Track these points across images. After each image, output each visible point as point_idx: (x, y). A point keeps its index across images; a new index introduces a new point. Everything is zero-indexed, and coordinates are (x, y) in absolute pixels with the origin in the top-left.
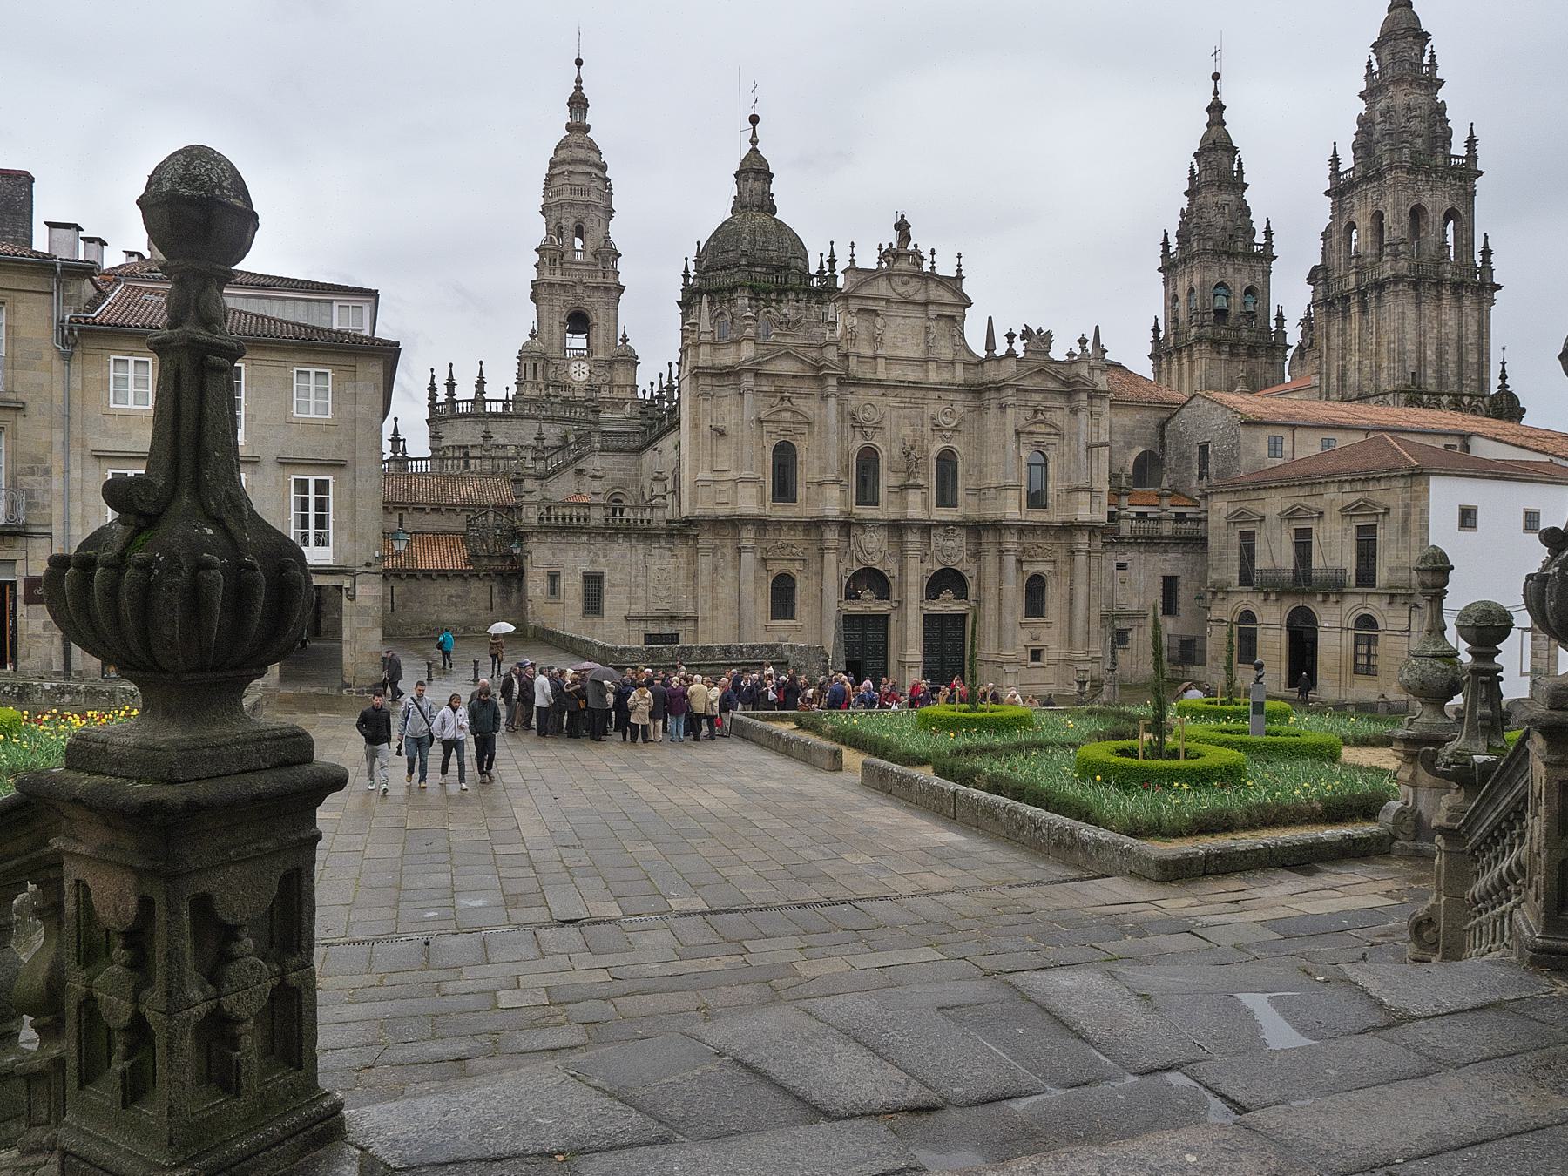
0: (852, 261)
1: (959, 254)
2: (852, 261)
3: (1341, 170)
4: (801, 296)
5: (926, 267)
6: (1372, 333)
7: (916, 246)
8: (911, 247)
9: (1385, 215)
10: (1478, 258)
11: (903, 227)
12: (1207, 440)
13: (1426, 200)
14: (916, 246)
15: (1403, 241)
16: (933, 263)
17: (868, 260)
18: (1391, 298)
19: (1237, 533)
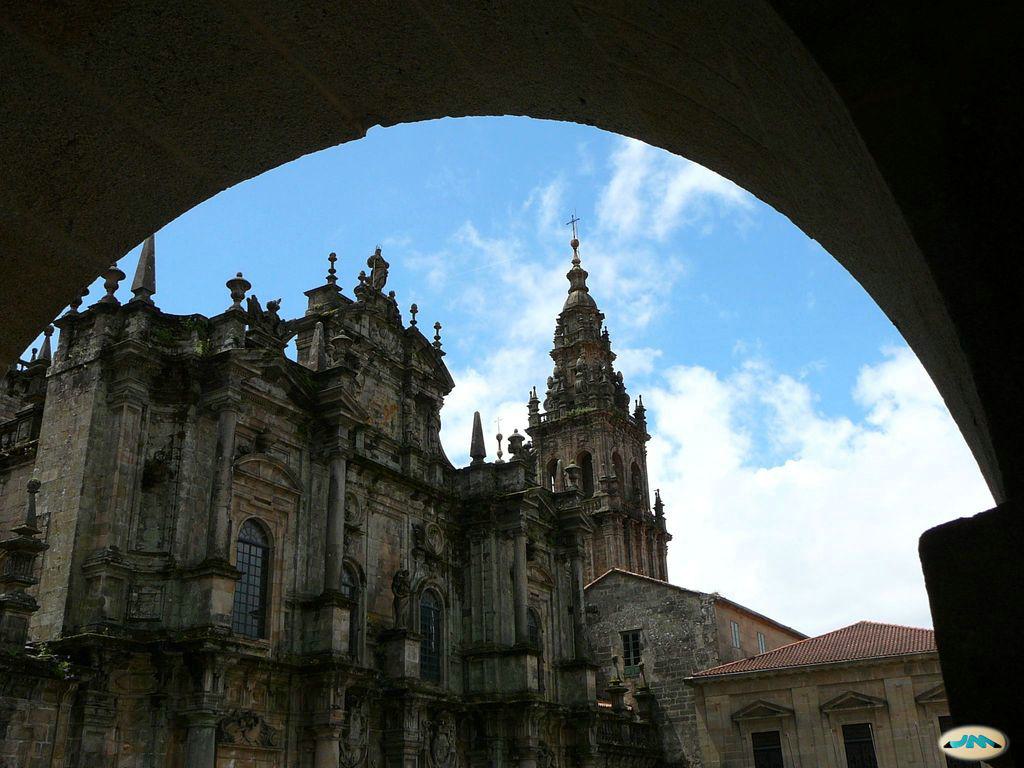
0: (332, 278)
1: (438, 324)
2: (332, 278)
3: (540, 412)
4: (17, 387)
5: (406, 325)
6: (589, 564)
7: (392, 294)
8: (386, 291)
9: (593, 457)
10: (654, 512)
11: (378, 264)
12: (635, 627)
13: (621, 449)
14: (392, 294)
15: (615, 481)
16: (414, 322)
17: (348, 288)
18: (611, 531)
19: (749, 737)
